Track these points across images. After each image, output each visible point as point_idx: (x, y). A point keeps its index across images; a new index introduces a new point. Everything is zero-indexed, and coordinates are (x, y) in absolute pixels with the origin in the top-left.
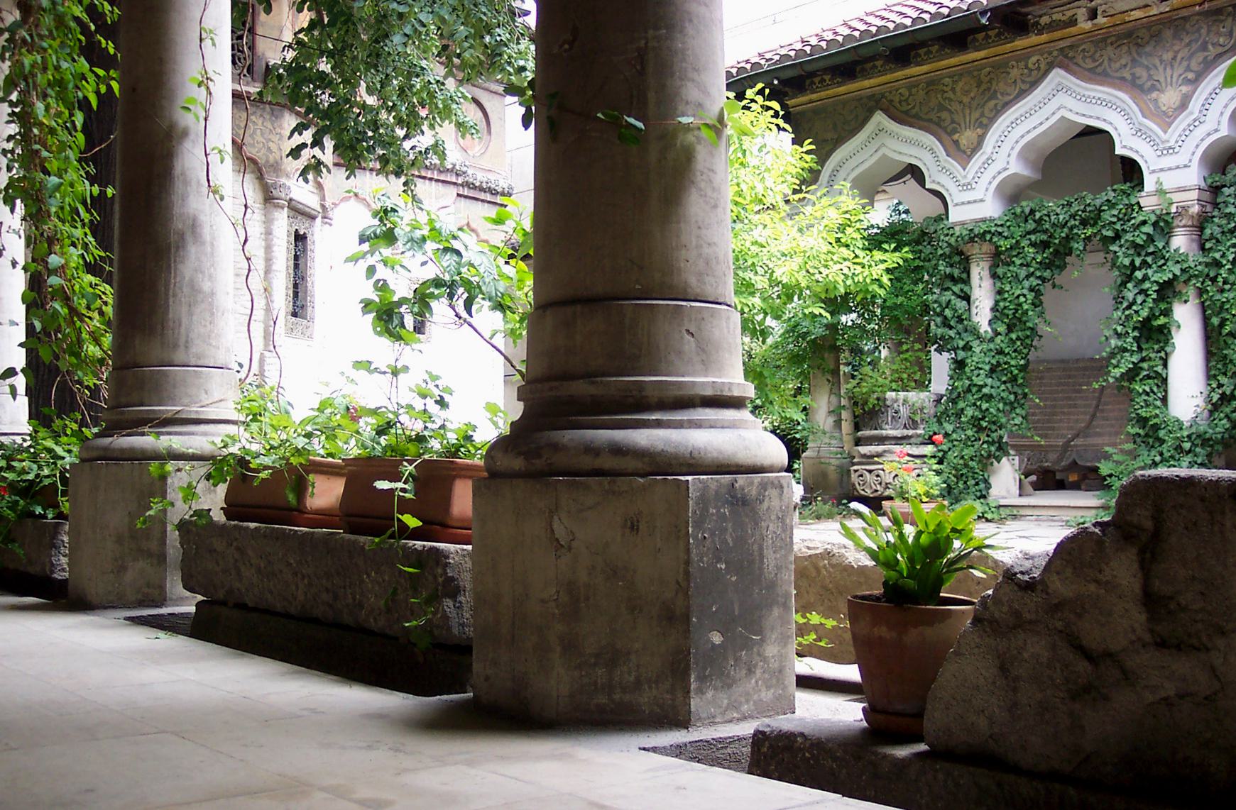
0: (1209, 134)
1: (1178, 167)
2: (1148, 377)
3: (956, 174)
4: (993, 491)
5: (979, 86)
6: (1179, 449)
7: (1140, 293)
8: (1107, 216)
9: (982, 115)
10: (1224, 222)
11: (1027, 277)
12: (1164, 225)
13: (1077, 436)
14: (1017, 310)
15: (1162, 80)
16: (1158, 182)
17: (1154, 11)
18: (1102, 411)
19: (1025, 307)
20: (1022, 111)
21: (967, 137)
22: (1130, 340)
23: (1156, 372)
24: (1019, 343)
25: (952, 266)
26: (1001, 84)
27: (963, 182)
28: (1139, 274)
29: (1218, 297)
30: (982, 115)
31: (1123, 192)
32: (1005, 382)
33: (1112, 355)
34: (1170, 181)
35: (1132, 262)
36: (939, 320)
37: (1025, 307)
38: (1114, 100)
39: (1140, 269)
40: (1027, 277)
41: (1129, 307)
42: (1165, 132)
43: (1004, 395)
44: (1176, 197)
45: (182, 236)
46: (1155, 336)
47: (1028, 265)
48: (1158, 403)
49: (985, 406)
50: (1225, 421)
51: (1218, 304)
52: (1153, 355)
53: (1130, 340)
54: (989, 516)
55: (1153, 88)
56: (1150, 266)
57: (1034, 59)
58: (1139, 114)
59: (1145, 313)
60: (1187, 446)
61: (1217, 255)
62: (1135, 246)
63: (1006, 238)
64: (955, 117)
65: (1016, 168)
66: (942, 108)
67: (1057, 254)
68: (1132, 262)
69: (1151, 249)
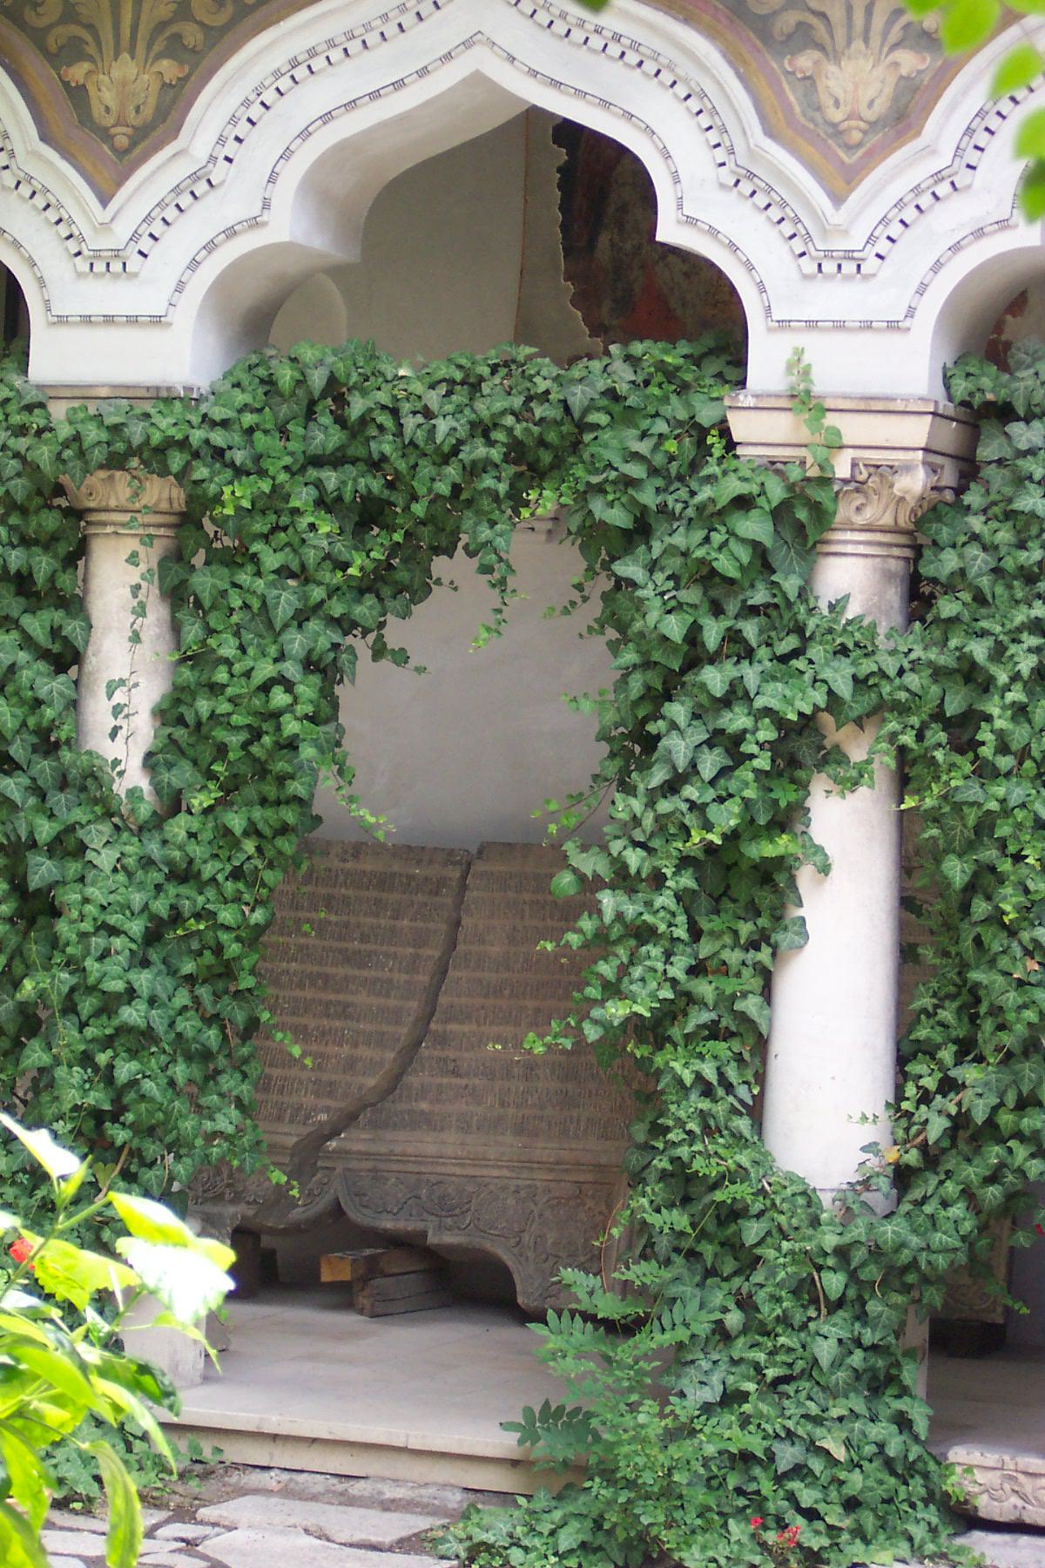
0: (979, 233)
1: (867, 326)
2: (714, 1032)
3: (71, 209)
6: (807, 1291)
7: (709, 743)
8: (614, 446)
10: (1004, 535)
11: (301, 618)
13: (348, 1119)
14: (256, 735)
15: (837, 14)
16: (798, 366)
18: (443, 1040)
19: (291, 726)
21: (121, 82)
22: (665, 899)
23: (743, 1018)
24: (249, 846)
25: (26, 542)
27: (95, 242)
28: (714, 678)
29: (973, 792)
31: (670, 374)
32: (190, 980)
33: (601, 942)
34: (839, 368)
35: (694, 635)
37: (291, 726)
38: (668, 53)
39: (713, 659)
40: (301, 618)
41: (672, 787)
42: (838, 200)
43: (188, 1025)
44: (854, 429)
46: (742, 890)
47: (303, 575)
48: (743, 1124)
50: (958, 1210)
51: (972, 817)
52: (733, 957)
53: (665, 899)
55: (803, 38)
56: (749, 654)
59: (727, 817)
60: (834, 1283)
61: (979, 650)
62: (708, 576)
63: (240, 472)
67: (400, 532)
68: (694, 635)
69: (760, 597)
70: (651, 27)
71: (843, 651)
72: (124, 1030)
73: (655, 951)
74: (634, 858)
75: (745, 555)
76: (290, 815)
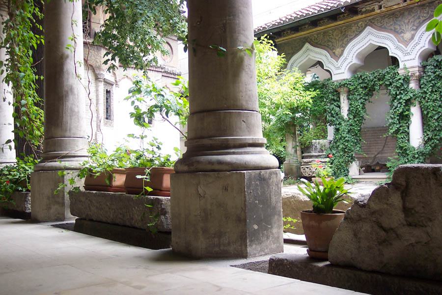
1: (411, 60)
2: (403, 132)
4: (350, 174)
5: (341, 33)
6: (414, 157)
8: (387, 77)
9: (343, 43)
10: (427, 78)
11: (360, 99)
12: (407, 80)
13: (378, 153)
15: (405, 29)
16: (405, 65)
17: (401, 6)
19: (359, 109)
20: (357, 41)
21: (337, 51)
25: (334, 96)
26: (349, 32)
27: (337, 66)
28: (398, 97)
30: (343, 43)
34: (408, 64)
36: (330, 115)
37: (359, 109)
39: (399, 95)
40: (360, 99)
41: (395, 108)
43: (353, 140)
44: (411, 70)
45: (67, 92)
47: (360, 95)
48: (406, 141)
49: (346, 144)
50: (430, 147)
51: (426, 106)
54: (349, 182)
55: (402, 32)
56: (402, 94)
57: (360, 23)
58: (397, 42)
59: (401, 110)
60: (417, 156)
61: (425, 90)
62: (397, 87)
63: (352, 86)
64: (334, 44)
65: (355, 61)
66: (329, 41)
67: (370, 91)
69: (403, 88)
70: (387, 35)
71: (412, 92)
72: (346, 140)
73: (395, 125)
74: (392, 116)
75: (400, 84)
76: (361, 118)
